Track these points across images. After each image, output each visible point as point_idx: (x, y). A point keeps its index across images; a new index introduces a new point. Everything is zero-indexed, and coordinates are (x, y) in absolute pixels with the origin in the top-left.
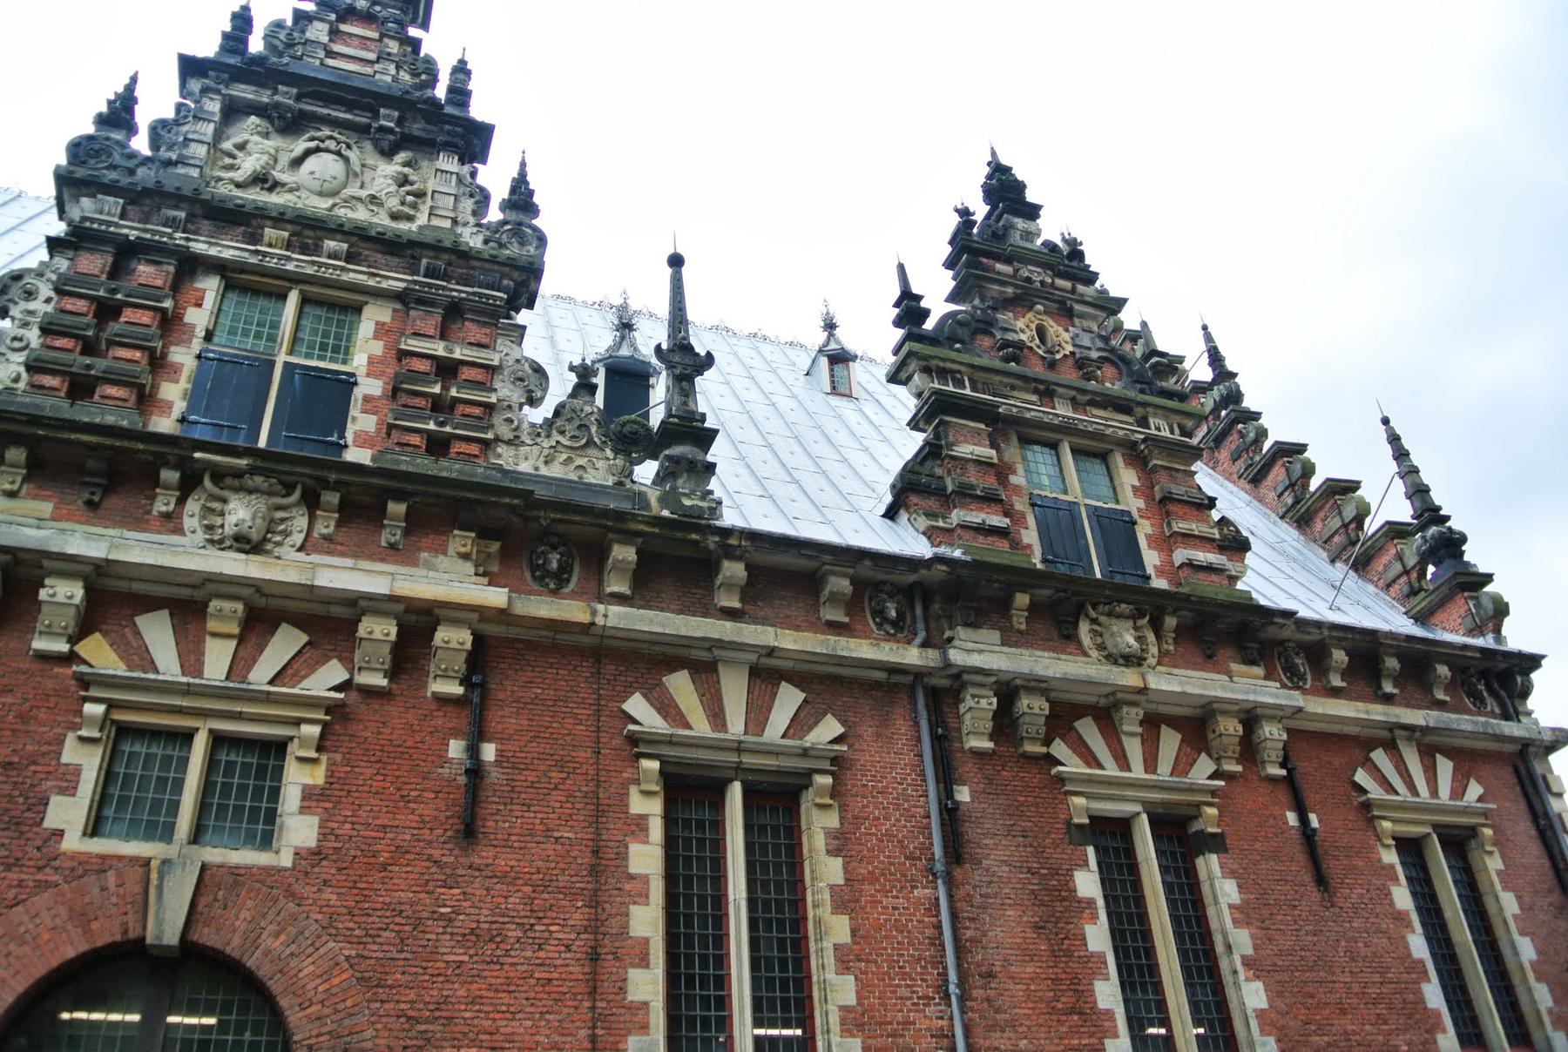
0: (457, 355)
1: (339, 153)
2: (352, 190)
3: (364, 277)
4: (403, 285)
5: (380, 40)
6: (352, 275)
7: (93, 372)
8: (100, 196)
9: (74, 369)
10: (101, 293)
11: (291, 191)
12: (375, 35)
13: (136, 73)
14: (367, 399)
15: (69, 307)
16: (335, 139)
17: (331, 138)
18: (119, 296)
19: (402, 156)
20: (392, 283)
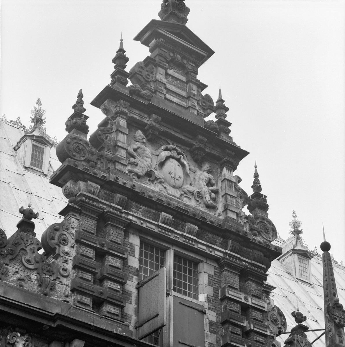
0: (250, 303)
1: (179, 160)
2: (187, 187)
3: (204, 248)
4: (221, 255)
5: (187, 83)
6: (200, 246)
7: (103, 297)
8: (90, 182)
9: (95, 294)
10: (98, 246)
11: (161, 183)
12: (184, 79)
13: (81, 90)
14: (211, 323)
15: (85, 253)
16: (176, 150)
17: (174, 149)
18: (105, 249)
19: (206, 166)
20: (217, 253)
